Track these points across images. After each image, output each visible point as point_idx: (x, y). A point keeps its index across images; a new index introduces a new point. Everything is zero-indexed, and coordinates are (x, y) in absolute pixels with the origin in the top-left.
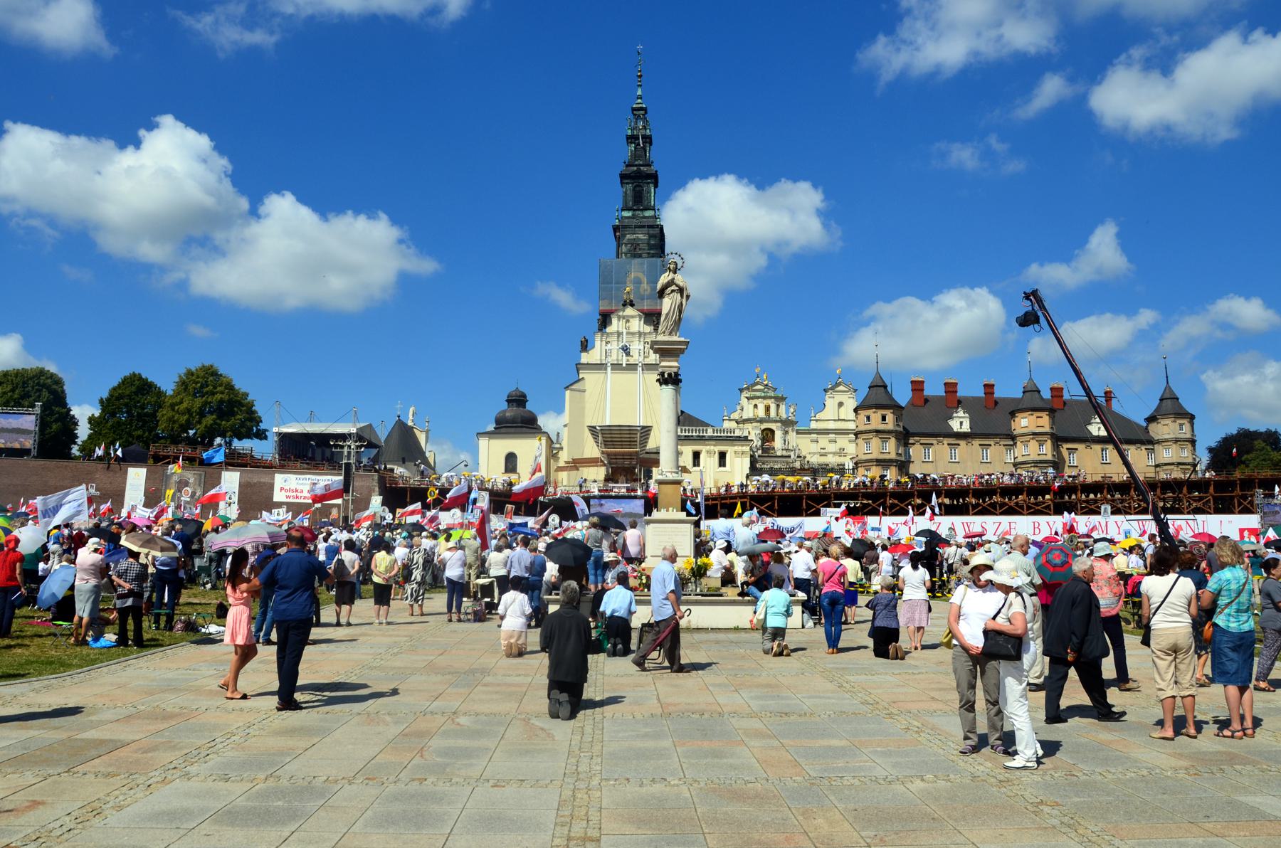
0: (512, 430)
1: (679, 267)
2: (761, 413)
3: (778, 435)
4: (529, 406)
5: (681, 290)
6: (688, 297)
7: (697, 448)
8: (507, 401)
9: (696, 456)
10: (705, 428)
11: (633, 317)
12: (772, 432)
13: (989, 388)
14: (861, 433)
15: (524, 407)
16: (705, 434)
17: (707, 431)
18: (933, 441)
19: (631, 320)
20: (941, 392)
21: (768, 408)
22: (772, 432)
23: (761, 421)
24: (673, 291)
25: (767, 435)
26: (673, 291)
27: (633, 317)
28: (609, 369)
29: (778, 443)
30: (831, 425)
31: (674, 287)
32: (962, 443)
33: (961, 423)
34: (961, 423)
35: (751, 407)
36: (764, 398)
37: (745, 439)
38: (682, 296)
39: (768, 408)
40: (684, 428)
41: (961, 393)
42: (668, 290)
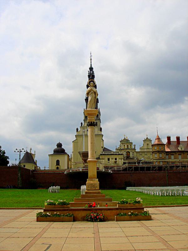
0: (58, 154)
2: (126, 147)
3: (131, 153)
4: (63, 147)
7: (109, 157)
12: (129, 152)
14: (154, 152)
15: (61, 147)
18: (174, 154)
21: (128, 146)
22: (129, 152)
23: (126, 149)
28: (84, 136)
29: (131, 156)
30: (145, 150)
32: (182, 154)
33: (182, 148)
34: (182, 148)
35: (123, 146)
36: (127, 143)
37: (122, 154)
39: (128, 146)
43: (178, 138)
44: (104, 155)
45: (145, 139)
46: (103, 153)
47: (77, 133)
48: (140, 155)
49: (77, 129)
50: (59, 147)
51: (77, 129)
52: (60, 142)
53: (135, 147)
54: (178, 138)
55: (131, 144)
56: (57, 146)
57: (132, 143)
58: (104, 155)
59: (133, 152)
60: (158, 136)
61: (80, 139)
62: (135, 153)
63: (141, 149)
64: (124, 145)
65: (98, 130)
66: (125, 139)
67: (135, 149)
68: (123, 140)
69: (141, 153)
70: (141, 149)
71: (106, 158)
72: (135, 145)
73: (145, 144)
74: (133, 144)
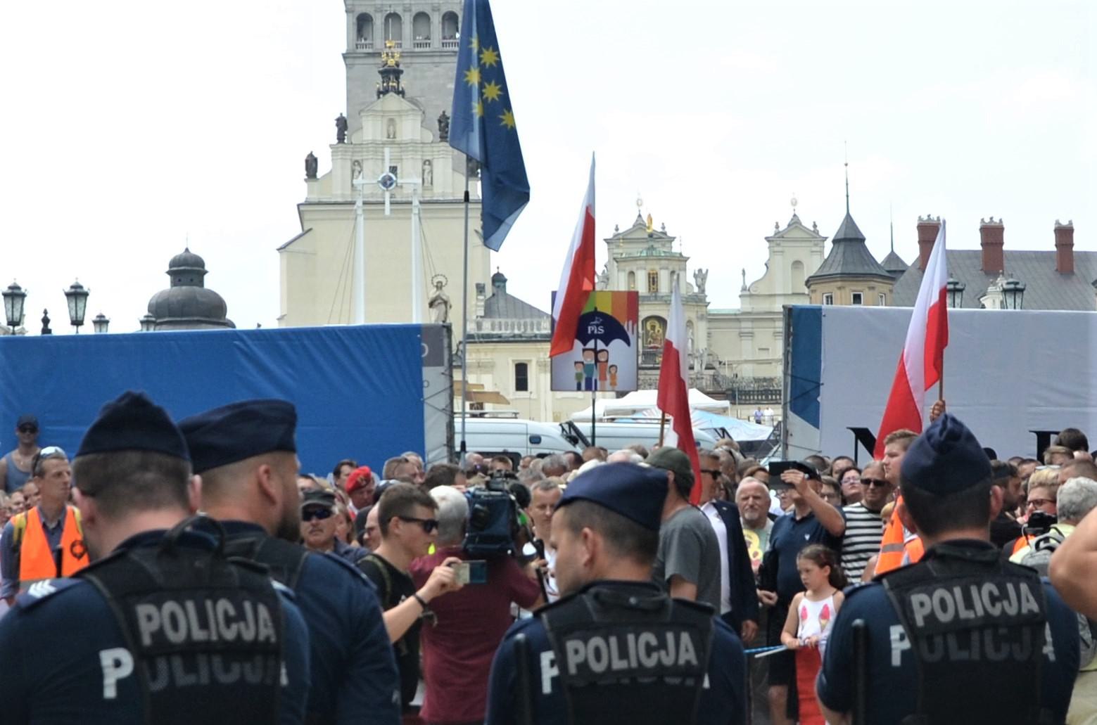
1: (444, 284)
4: (210, 283)
5: (445, 303)
6: (451, 307)
7: (522, 358)
8: (169, 273)
9: (521, 370)
10: (535, 321)
11: (400, 113)
13: (1064, 234)
15: (201, 283)
16: (536, 332)
17: (539, 324)
19: (397, 120)
20: (974, 243)
21: (653, 280)
24: (439, 303)
25: (653, 327)
26: (439, 303)
27: (400, 113)
31: (440, 301)
38: (446, 307)
39: (653, 280)
40: (497, 320)
41: (1011, 243)
42: (436, 303)
43: (992, 234)
44: (488, 339)
45: (783, 227)
46: (487, 328)
47: (310, 191)
48: (741, 335)
49: (312, 164)
50: (191, 283)
51: (312, 164)
52: (193, 251)
53: (701, 288)
54: (992, 234)
55: (674, 265)
56: (169, 273)
57: (682, 259)
58: (488, 339)
59: (690, 323)
60: (849, 221)
61: (329, 230)
62: (701, 328)
63: (747, 294)
64: (632, 273)
65: (454, 170)
66: (640, 225)
67: (698, 300)
68: (629, 232)
69: (746, 326)
70: (751, 296)
71: (506, 358)
72: (701, 276)
73: (778, 258)
74: (691, 267)
